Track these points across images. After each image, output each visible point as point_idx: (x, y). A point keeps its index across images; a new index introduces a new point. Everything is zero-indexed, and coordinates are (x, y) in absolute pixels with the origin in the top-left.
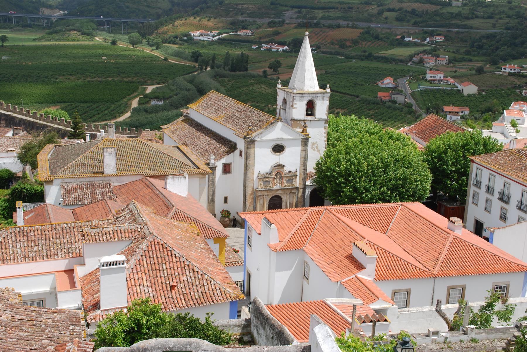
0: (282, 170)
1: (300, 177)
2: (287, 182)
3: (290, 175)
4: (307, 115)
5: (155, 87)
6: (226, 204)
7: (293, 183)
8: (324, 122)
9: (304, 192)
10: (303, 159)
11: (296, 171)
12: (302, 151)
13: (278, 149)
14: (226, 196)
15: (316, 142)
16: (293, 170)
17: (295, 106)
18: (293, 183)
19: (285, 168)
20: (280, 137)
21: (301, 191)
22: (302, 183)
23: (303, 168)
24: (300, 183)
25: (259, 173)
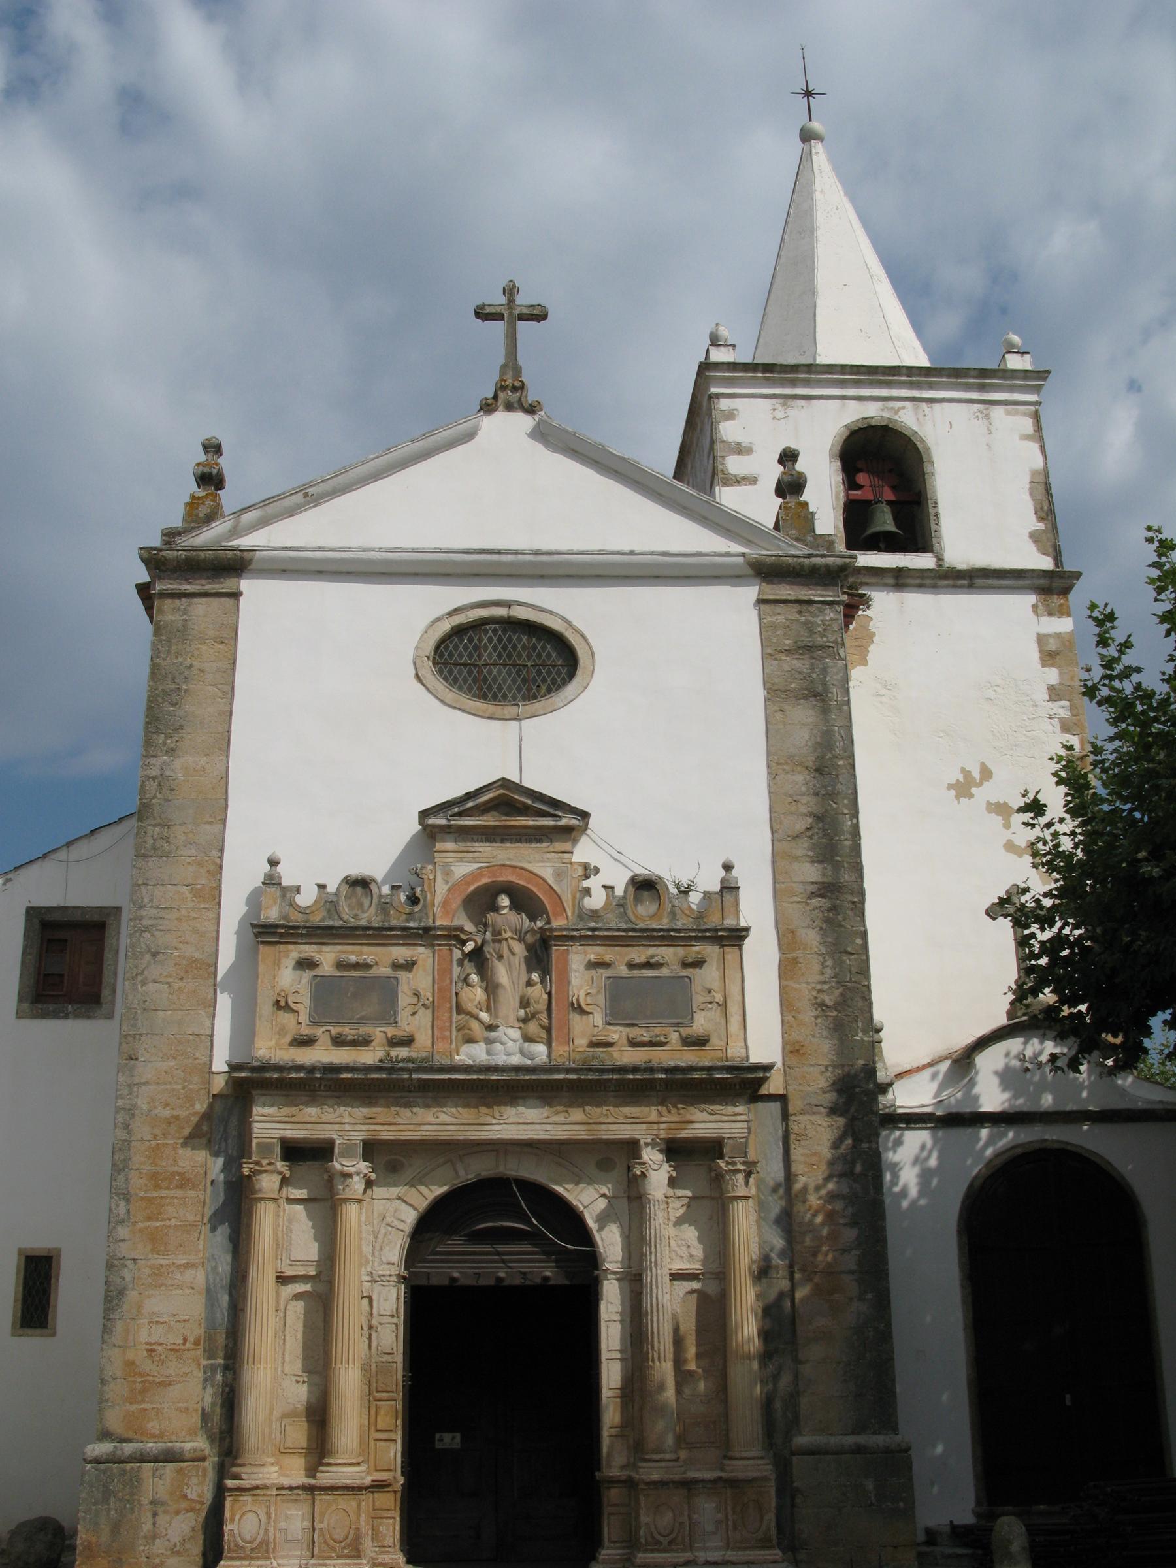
1: (788, 969)
2: (615, 1016)
3: (645, 912)
6: (33, 1343)
9: (860, 1167)
10: (800, 780)
12: (774, 692)
14: (39, 1243)
15: (986, 774)
17: (734, 465)
18: (701, 1023)
19: (583, 851)
21: (818, 1136)
22: (823, 1048)
23: (810, 873)
25: (271, 881)
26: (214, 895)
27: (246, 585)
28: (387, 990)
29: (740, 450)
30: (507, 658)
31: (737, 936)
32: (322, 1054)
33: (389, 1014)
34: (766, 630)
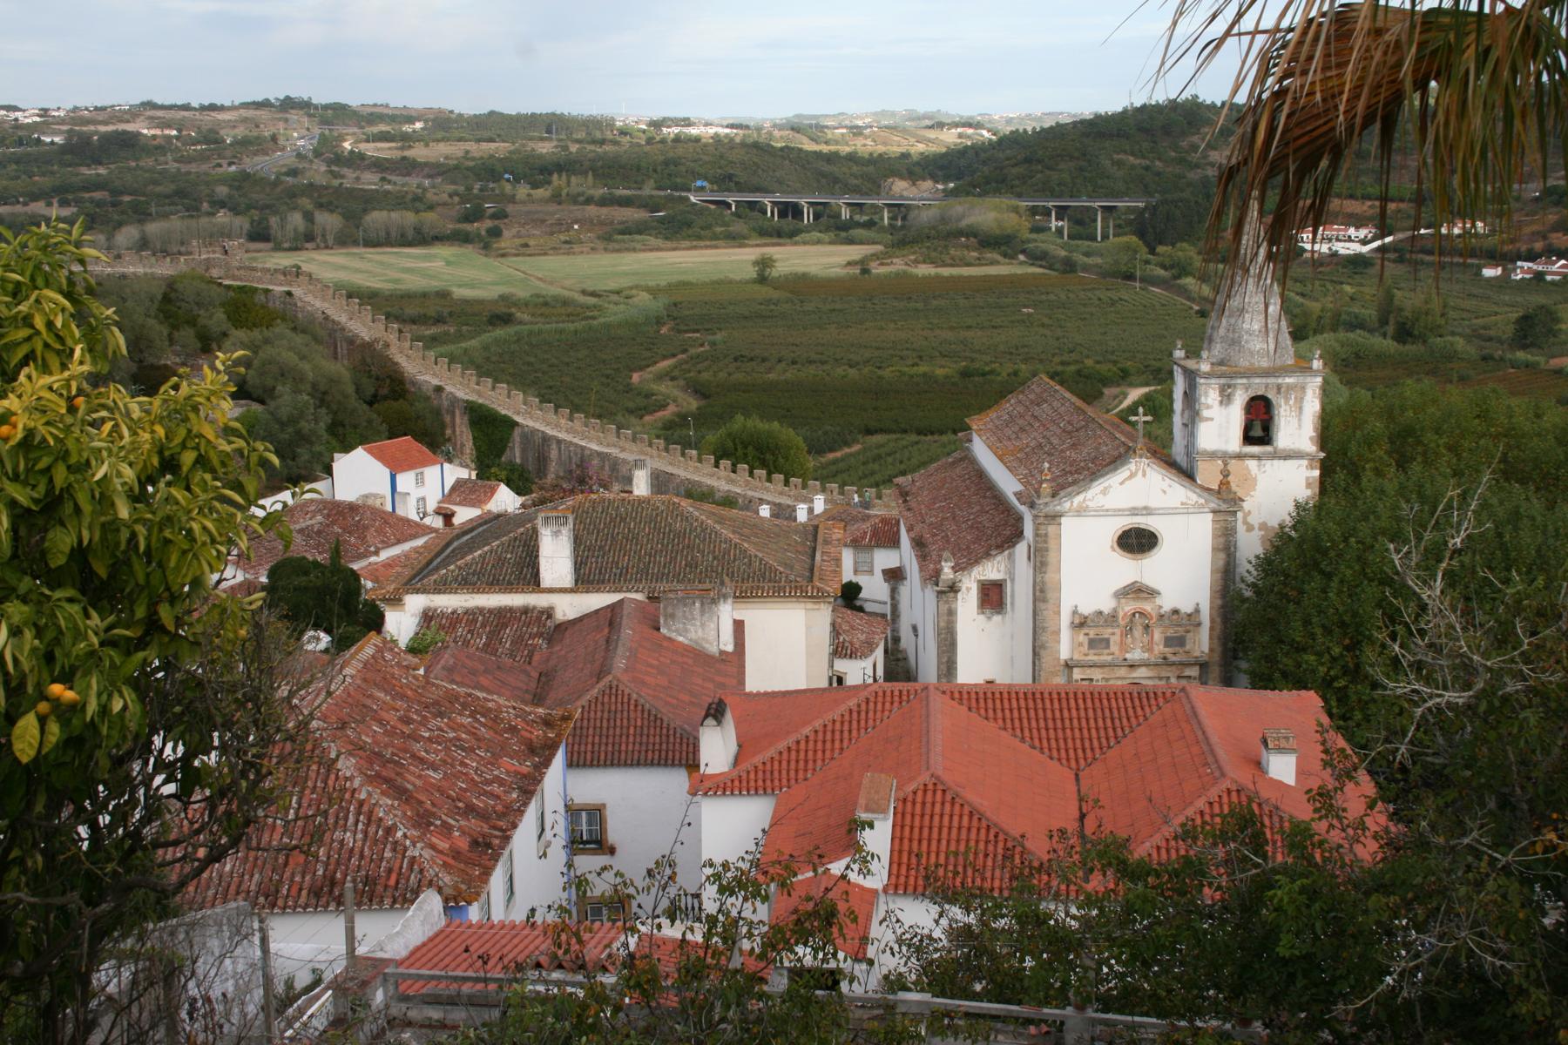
0: (1148, 607)
1: (1212, 629)
2: (1166, 646)
4: (1248, 439)
5: (1145, 390)
7: (1188, 647)
8: (1305, 462)
11: (1197, 611)
13: (1137, 541)
16: (1187, 608)
17: (1205, 413)
19: (1158, 601)
20: (1140, 504)
22: (1218, 649)
23: (1219, 602)
24: (1211, 650)
25: (1075, 612)
26: (1059, 613)
27: (1063, 520)
28: (1107, 641)
29: (1209, 407)
30: (1137, 541)
31: (1199, 624)
32: (1092, 658)
33: (1108, 646)
34: (1214, 529)
